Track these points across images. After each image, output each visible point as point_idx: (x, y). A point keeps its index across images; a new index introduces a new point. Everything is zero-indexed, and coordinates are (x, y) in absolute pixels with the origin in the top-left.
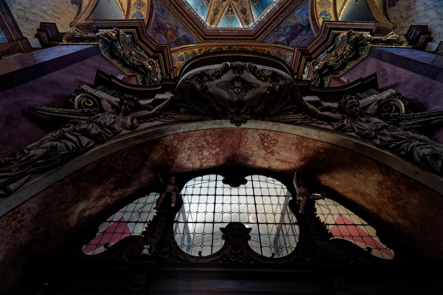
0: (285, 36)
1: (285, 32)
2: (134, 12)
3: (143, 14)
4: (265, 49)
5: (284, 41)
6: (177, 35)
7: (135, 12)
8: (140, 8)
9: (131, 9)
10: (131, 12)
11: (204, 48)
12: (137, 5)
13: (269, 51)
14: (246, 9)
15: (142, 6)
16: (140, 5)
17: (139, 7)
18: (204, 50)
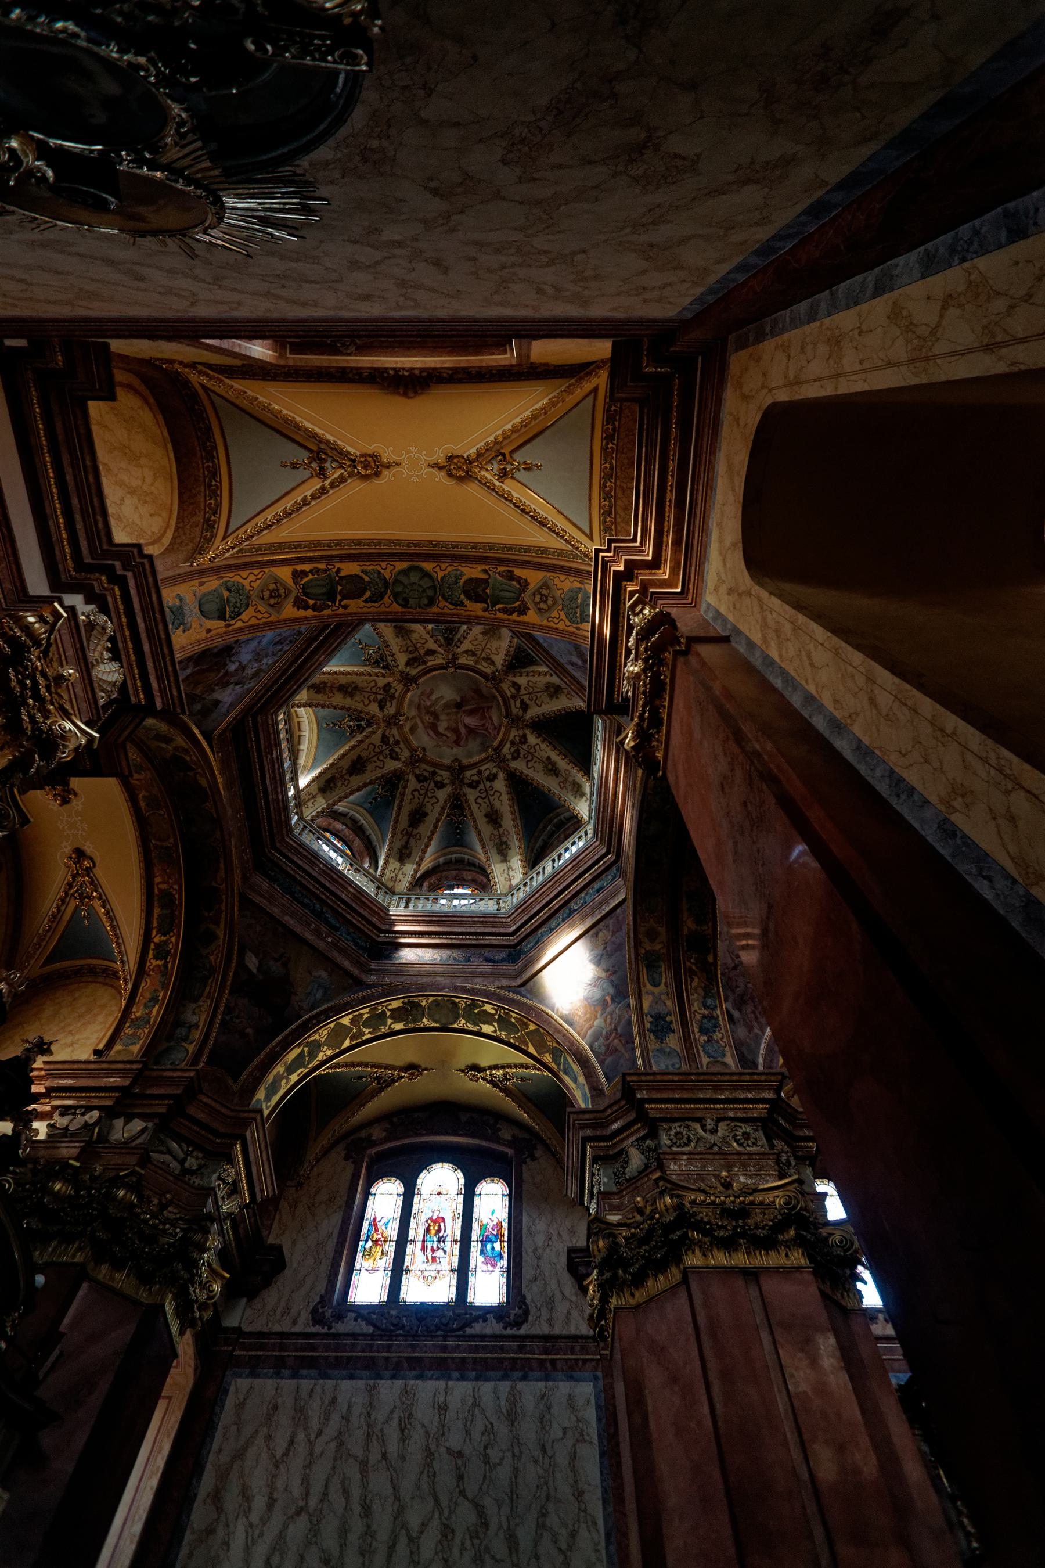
0: (259, 969)
1: (272, 963)
2: (246, 583)
3: (244, 616)
4: (222, 926)
5: (247, 969)
6: (213, 691)
7: (248, 588)
8: (263, 599)
9: (256, 572)
10: (244, 574)
11: (194, 758)
12: (272, 587)
13: (217, 937)
14: (364, 772)
15: (272, 606)
16: (274, 597)
17: (267, 594)
18: (188, 758)
